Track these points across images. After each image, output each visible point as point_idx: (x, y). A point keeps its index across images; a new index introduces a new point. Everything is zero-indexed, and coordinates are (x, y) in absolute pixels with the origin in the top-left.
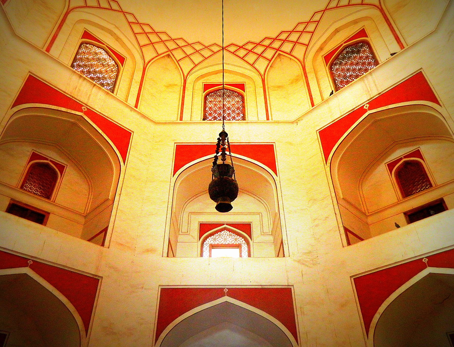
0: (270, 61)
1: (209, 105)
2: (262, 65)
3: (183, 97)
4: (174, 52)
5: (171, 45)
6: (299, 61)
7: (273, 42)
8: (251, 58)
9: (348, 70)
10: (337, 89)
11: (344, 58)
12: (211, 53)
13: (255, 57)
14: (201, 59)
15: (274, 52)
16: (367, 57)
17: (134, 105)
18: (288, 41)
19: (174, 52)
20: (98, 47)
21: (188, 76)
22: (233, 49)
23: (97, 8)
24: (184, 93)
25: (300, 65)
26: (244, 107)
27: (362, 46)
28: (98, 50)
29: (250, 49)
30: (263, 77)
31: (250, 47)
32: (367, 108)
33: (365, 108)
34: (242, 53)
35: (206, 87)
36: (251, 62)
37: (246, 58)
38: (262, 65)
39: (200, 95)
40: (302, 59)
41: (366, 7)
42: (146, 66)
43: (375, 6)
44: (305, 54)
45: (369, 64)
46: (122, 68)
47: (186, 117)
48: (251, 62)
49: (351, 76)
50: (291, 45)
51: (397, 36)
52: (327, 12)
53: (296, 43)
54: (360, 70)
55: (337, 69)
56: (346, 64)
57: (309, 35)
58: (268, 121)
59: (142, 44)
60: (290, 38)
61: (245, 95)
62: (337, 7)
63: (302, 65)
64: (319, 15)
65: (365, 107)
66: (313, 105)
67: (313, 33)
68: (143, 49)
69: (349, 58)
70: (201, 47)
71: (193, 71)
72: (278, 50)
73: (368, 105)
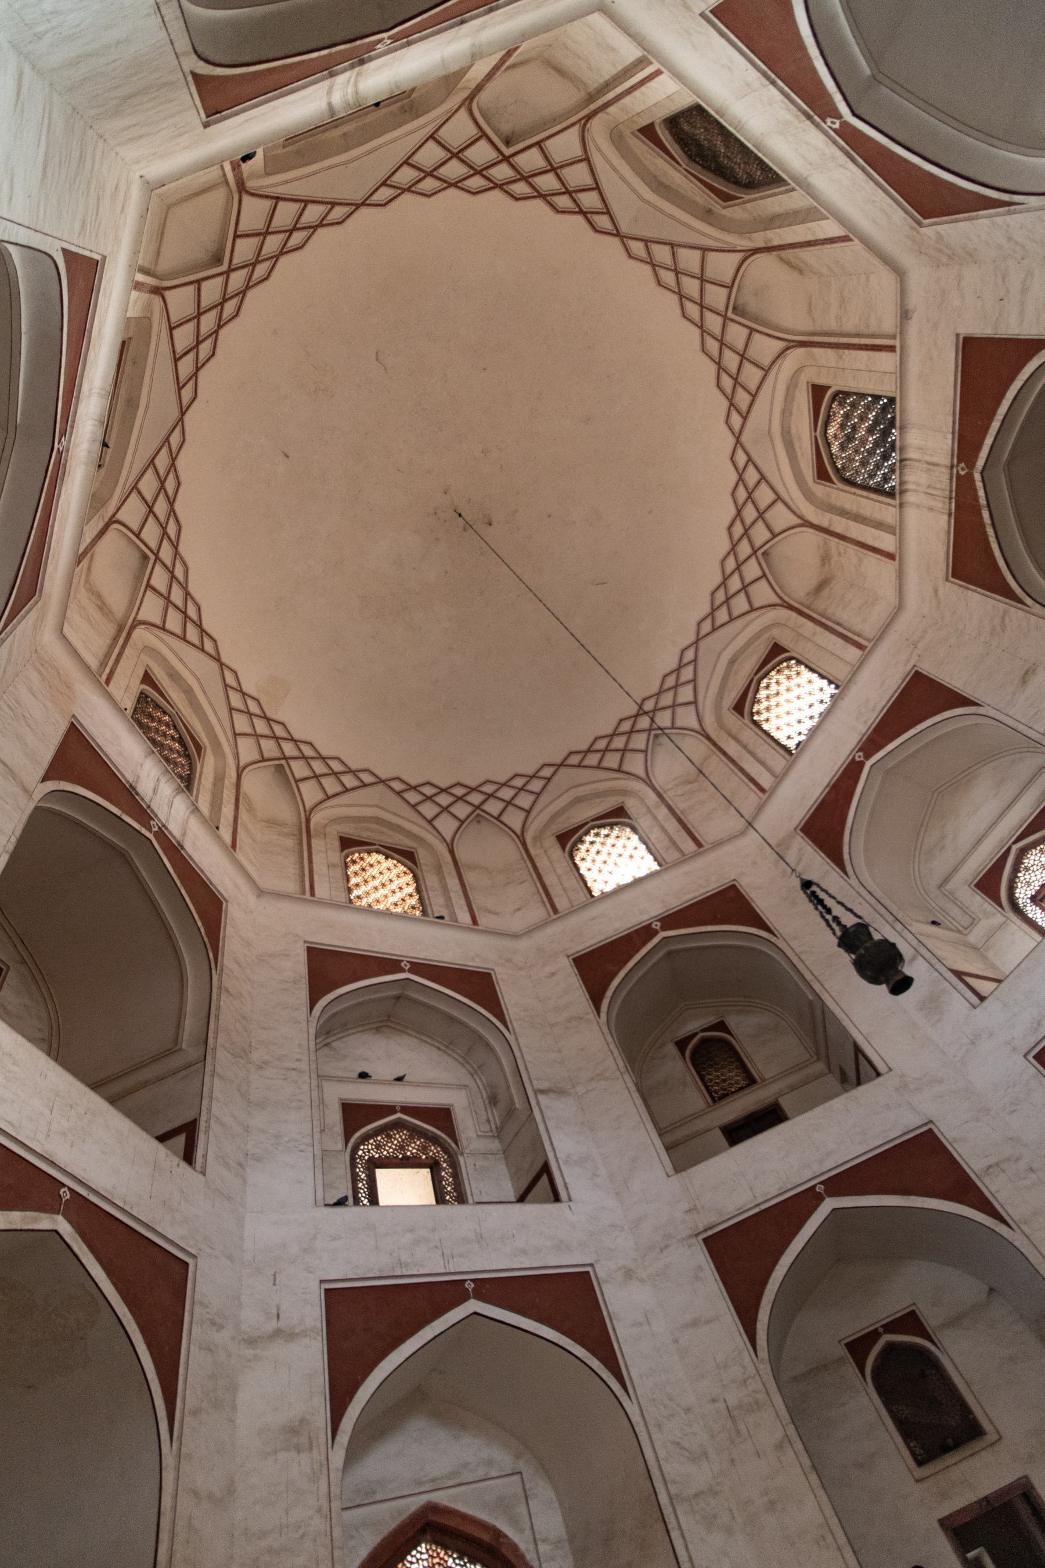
0: (538, 144)
4: (721, 308)
5: (714, 322)
7: (508, 183)
13: (565, 172)
15: (520, 160)
21: (739, 248)
22: (603, 221)
23: (767, 481)
29: (566, 197)
36: (583, 166)
37: (589, 181)
38: (565, 145)
41: (269, 190)
42: (793, 341)
44: (447, 120)
52: (359, 197)
59: (760, 373)
60: (463, 170)
61: (658, 121)
62: (334, 204)
64: (377, 197)
67: (406, 162)
68: (766, 362)
70: (662, 273)
72: (506, 159)
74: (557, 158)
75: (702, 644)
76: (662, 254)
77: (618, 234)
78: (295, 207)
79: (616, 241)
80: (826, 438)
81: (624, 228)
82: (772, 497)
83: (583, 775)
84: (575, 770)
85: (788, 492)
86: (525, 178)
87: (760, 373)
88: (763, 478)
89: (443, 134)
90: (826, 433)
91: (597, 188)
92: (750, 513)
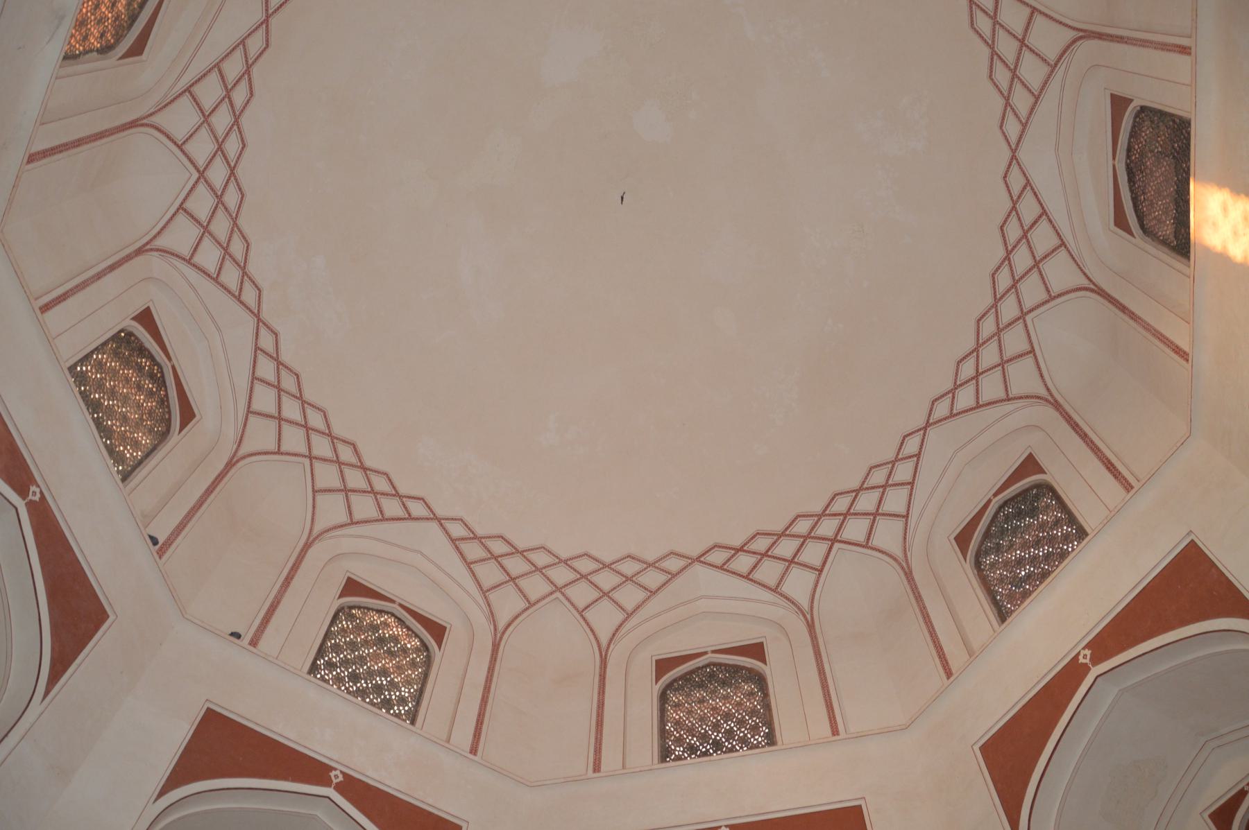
1: (673, 714)
2: (798, 584)
3: (601, 705)
6: (895, 559)
8: (769, 571)
9: (1020, 562)
10: (1003, 616)
11: (1003, 532)
12: (663, 578)
14: (641, 595)
16: (1057, 523)
17: (468, 749)
18: (855, 514)
19: (569, 591)
20: (380, 612)
22: (718, 557)
24: (602, 691)
25: (898, 568)
26: (767, 707)
27: (1037, 497)
28: (378, 619)
29: (763, 550)
30: (809, 617)
31: (761, 544)
32: (1087, 661)
33: (1081, 660)
34: (743, 563)
35: (663, 666)
36: (772, 583)
37: (756, 575)
39: (646, 692)
40: (898, 553)
43: (1038, 397)
45: (1066, 538)
46: (437, 654)
47: (610, 759)
48: (772, 583)
49: (1029, 576)
50: (865, 523)
51: (1109, 462)
53: (875, 515)
54: (1047, 557)
55: (993, 565)
56: (1011, 547)
57: (905, 491)
58: (836, 738)
59: (486, 584)
63: (903, 568)
65: (1081, 657)
66: (949, 674)
67: (912, 484)
69: (1015, 530)
71: (623, 630)
73: (1088, 652)
74: (795, 571)
75: (251, 322)
76: (653, 579)
77: (698, 559)
78: (985, 398)
79: (695, 554)
80: (387, 613)
81: (698, 567)
82: (357, 516)
83: (223, 36)
84: (243, 31)
85: (352, 536)
86: (806, 538)
87: (486, 584)
88: (384, 519)
89: (898, 524)
90: (393, 615)
91: (747, 577)
92: (355, 479)
